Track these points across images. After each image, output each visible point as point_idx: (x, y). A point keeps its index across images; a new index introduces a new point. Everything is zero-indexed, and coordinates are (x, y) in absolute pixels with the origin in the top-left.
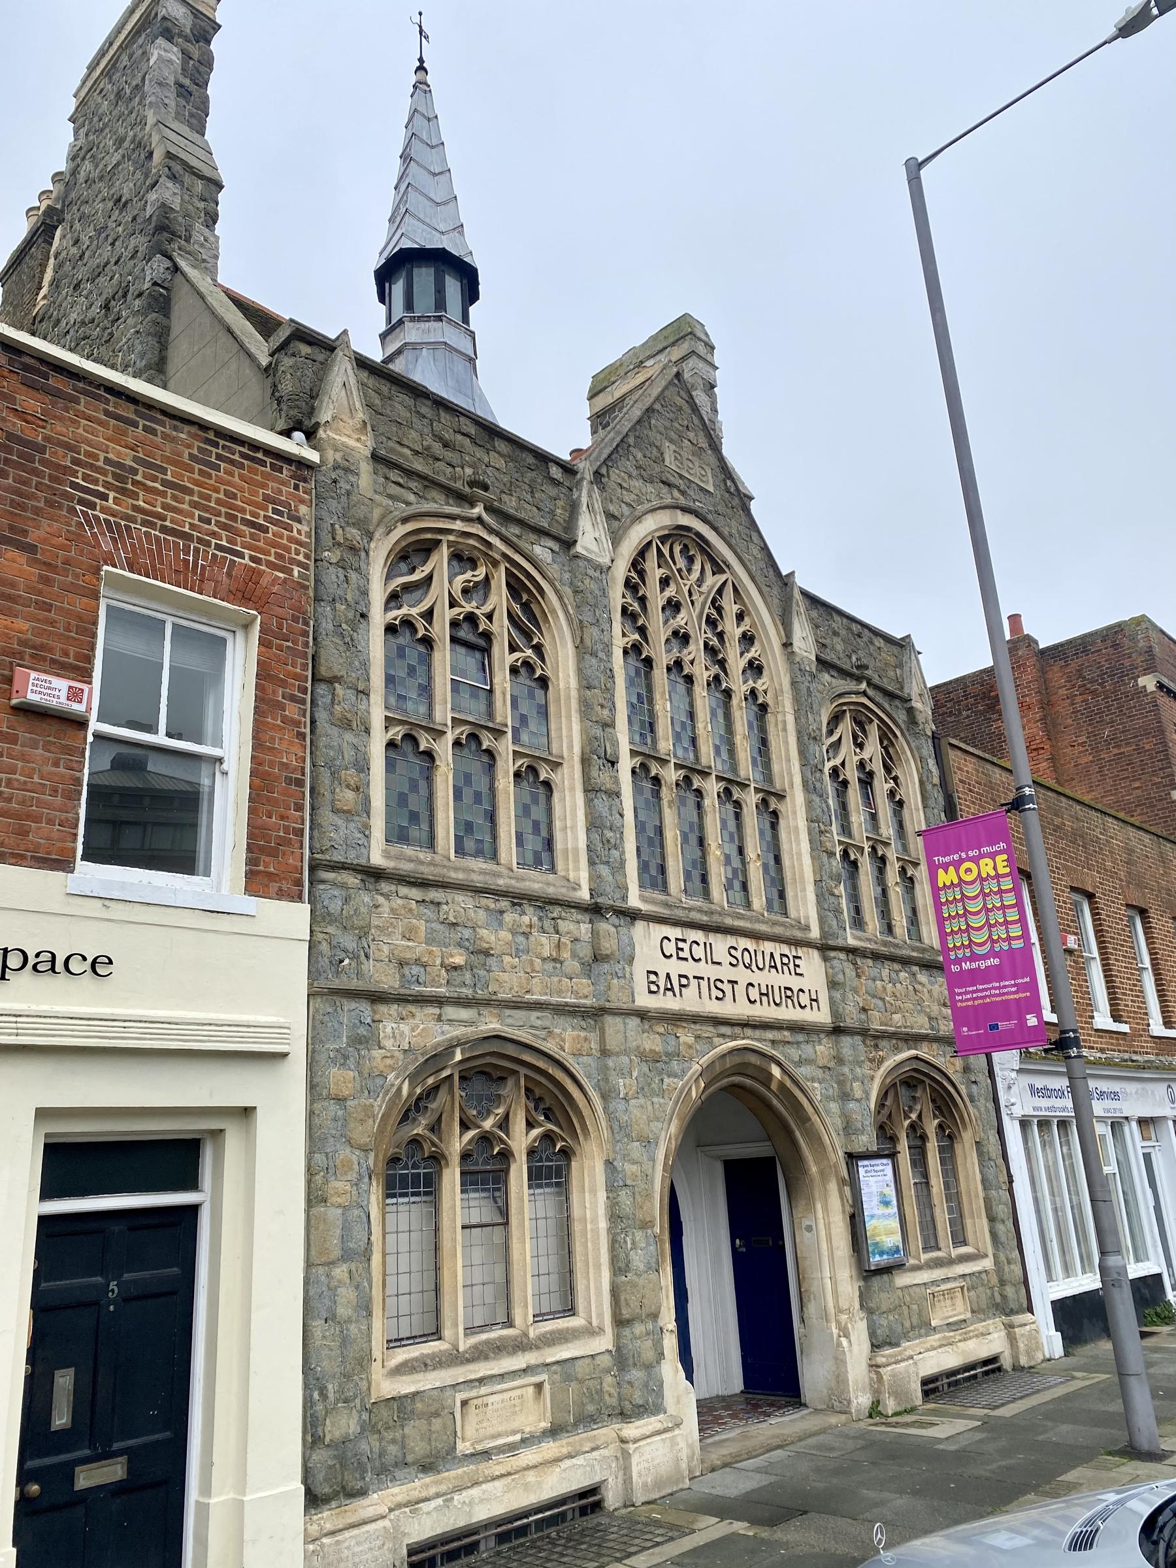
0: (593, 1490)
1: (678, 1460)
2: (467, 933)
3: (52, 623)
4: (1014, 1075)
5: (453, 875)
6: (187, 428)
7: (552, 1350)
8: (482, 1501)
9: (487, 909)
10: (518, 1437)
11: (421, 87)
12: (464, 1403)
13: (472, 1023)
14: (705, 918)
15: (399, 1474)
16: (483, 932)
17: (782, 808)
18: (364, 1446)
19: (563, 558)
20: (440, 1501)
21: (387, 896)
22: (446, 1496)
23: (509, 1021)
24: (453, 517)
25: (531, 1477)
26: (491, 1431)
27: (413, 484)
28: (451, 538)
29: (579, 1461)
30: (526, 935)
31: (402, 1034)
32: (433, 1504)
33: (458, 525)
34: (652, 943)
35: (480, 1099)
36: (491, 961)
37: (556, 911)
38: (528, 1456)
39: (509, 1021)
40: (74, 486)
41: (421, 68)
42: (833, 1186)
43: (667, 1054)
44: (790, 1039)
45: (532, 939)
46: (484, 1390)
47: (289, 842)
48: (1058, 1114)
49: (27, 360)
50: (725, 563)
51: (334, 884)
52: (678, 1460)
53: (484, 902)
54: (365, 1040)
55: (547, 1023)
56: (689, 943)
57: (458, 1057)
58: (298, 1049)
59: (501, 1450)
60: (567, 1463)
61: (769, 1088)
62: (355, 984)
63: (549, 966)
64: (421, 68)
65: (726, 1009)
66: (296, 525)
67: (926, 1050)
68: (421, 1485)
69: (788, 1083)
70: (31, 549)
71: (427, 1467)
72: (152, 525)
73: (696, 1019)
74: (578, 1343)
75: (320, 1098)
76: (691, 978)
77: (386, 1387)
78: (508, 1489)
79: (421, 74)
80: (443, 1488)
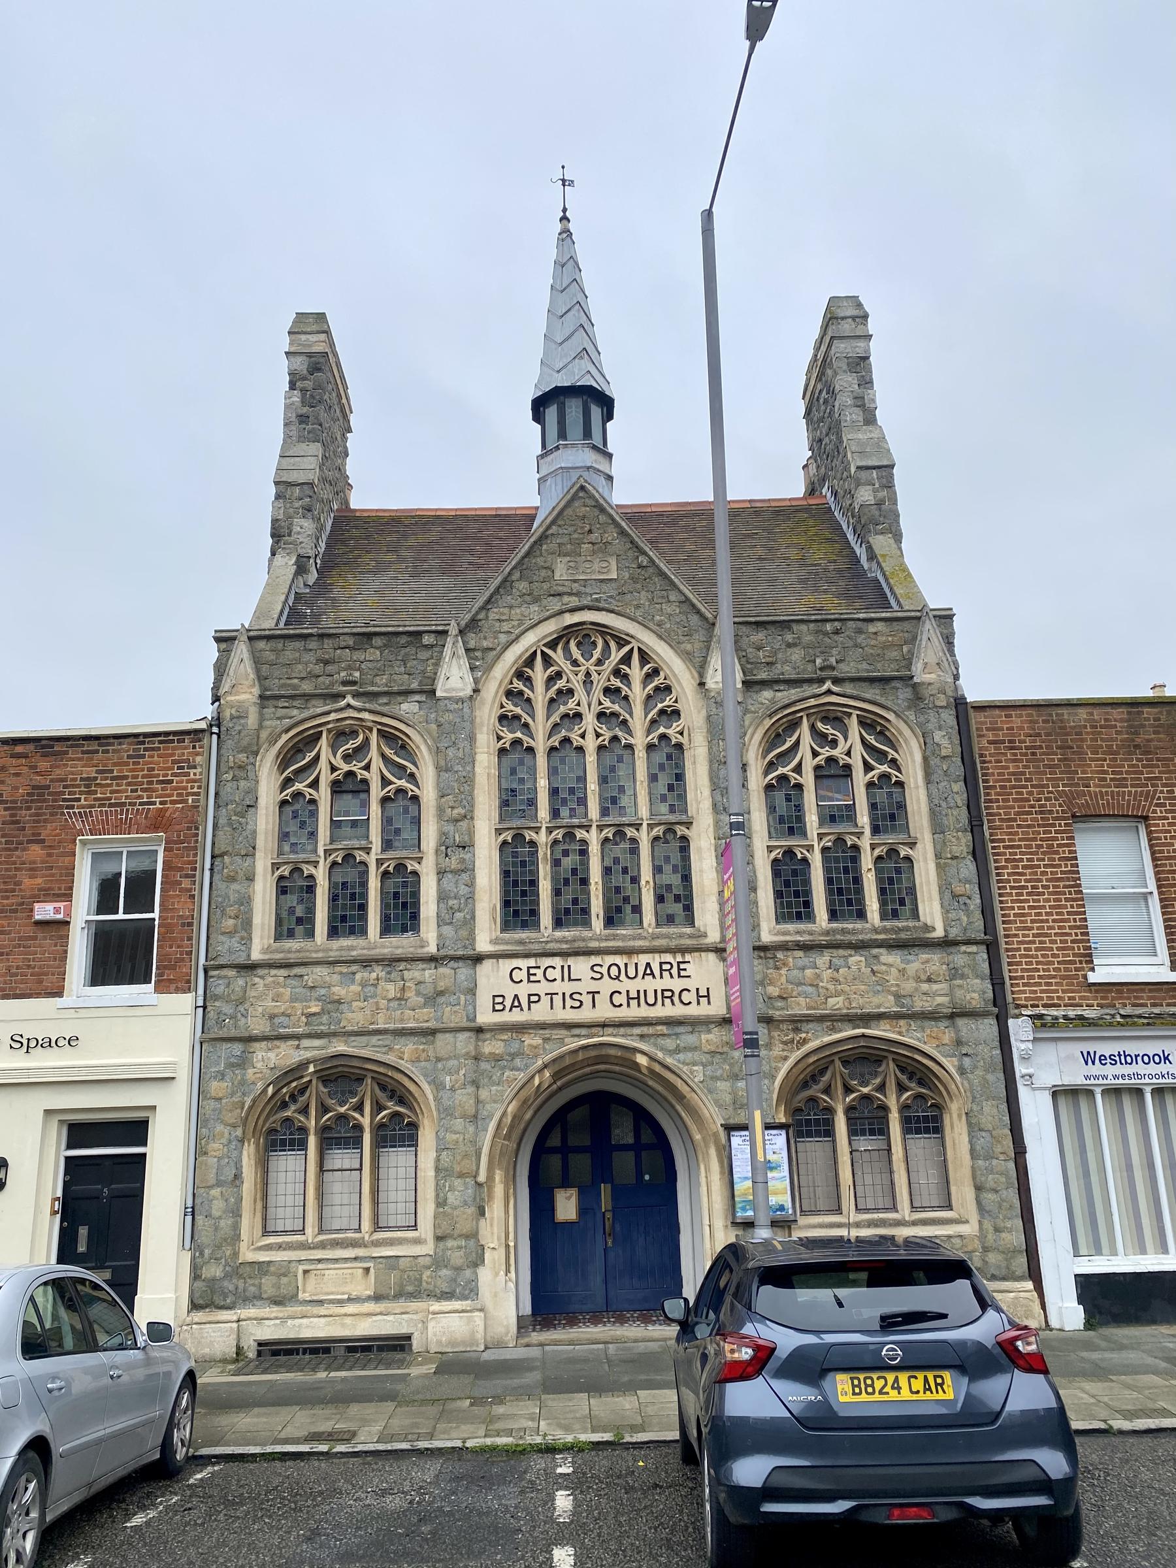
0: (408, 1338)
1: (473, 1333)
2: (323, 991)
3: (53, 875)
4: (1030, 1045)
5: (314, 955)
6: (127, 740)
7: (377, 1249)
8: (308, 1327)
9: (341, 973)
10: (346, 1297)
11: (566, 234)
12: (306, 1272)
13: (322, 1048)
14: (565, 946)
15: (258, 1303)
16: (335, 989)
17: (691, 833)
18: (226, 1283)
19: (430, 703)
20: (278, 1321)
21: (262, 977)
22: (284, 1320)
23: (354, 1044)
24: (328, 713)
25: (348, 1320)
26: (326, 1290)
27: (296, 703)
28: (330, 726)
29: (390, 1318)
30: (375, 986)
31: (269, 1058)
32: (272, 1322)
33: (333, 716)
34: (501, 974)
35: (343, 1093)
36: (344, 1007)
37: (402, 965)
38: (351, 1308)
39: (354, 1044)
40: (64, 800)
41: (564, 218)
42: (713, 1152)
43: (510, 1054)
44: (666, 1032)
45: (379, 987)
46: (320, 1266)
47: (183, 960)
48: (1101, 1081)
49: (44, 742)
50: (627, 635)
51: (219, 977)
52: (473, 1333)
53: (338, 969)
54: (243, 1063)
55: (387, 1043)
56: (542, 969)
57: (311, 1069)
58: (184, 1075)
59: (331, 1302)
60: (380, 1317)
61: (640, 1072)
62: (233, 1033)
63: (394, 1004)
64: (564, 218)
65: (586, 1014)
66: (192, 771)
67: (888, 1027)
68: (275, 1311)
69: (657, 1068)
70: (43, 841)
71: (278, 1302)
72: (103, 805)
73: (542, 1026)
74: (405, 1247)
75: (205, 1098)
76: (542, 995)
77: (248, 1255)
78: (328, 1324)
79: (565, 222)
80: (281, 1315)
